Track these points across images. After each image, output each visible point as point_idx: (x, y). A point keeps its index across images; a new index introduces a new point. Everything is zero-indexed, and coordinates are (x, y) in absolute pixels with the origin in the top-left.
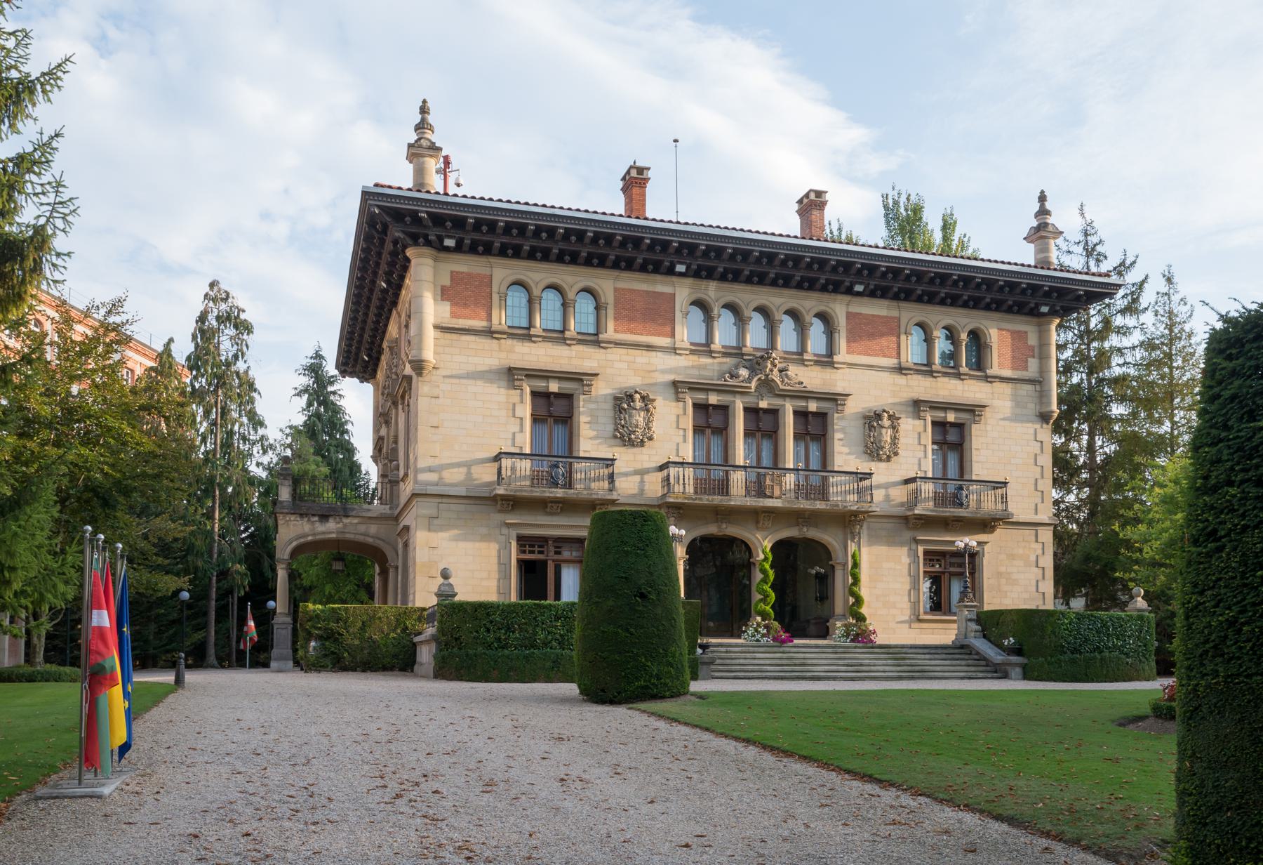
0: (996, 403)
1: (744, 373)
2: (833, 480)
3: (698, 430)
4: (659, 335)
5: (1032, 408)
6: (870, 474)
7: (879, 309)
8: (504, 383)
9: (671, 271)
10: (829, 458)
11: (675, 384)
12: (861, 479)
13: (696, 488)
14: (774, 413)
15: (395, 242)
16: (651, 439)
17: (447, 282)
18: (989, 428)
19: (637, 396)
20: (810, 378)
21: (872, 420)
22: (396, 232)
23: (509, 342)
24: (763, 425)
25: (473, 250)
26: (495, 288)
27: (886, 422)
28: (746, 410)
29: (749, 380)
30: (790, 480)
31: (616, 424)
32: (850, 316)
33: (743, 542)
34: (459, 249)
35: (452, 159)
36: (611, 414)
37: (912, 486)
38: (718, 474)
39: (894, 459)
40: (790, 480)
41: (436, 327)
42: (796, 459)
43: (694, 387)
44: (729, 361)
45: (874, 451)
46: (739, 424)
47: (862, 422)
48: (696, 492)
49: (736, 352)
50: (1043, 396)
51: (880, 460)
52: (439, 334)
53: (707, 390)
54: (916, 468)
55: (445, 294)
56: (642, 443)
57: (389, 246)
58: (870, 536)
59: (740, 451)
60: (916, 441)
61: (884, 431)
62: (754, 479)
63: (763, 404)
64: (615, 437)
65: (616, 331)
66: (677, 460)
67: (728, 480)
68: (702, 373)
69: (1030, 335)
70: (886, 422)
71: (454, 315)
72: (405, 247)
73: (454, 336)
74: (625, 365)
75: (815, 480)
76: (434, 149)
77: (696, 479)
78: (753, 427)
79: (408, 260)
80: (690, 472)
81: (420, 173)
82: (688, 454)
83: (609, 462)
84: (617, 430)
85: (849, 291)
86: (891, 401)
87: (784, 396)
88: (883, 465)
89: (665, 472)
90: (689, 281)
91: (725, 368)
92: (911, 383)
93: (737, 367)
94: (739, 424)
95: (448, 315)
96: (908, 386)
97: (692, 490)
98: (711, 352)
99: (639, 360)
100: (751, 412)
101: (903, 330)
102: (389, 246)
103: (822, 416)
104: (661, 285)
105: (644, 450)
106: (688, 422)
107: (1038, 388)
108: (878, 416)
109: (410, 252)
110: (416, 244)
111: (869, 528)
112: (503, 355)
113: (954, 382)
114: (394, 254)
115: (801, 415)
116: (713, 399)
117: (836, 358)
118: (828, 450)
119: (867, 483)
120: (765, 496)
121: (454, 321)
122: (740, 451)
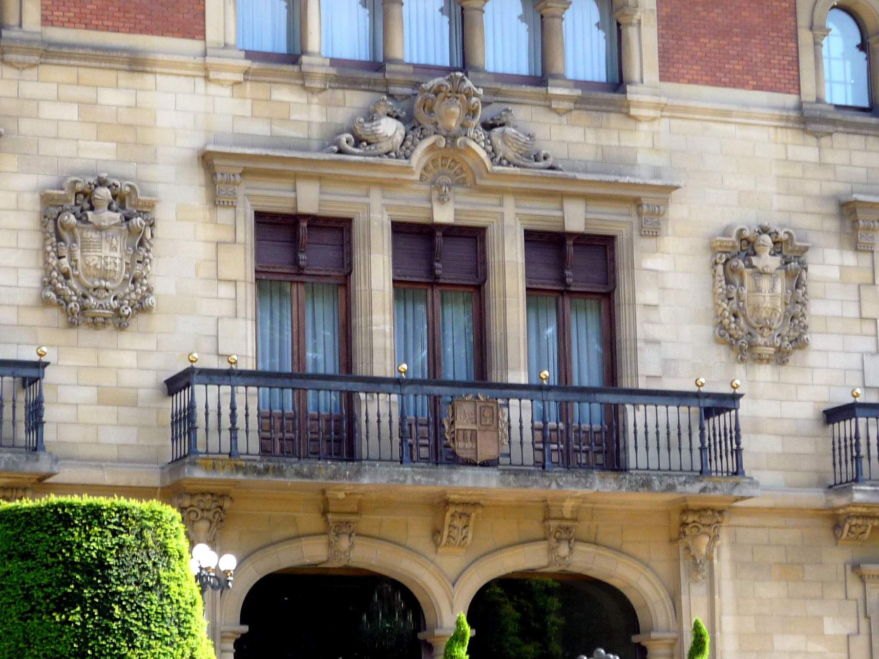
1: (389, 129)
2: (638, 417)
3: (267, 282)
4: (163, 32)
6: (735, 398)
10: (625, 356)
11: (207, 161)
12: (708, 413)
14: (473, 236)
16: (141, 308)
19: (104, 193)
20: (567, 137)
21: (735, 254)
24: (441, 260)
27: (768, 261)
28: (400, 229)
29: (405, 150)
30: (520, 413)
31: (47, 269)
33: (398, 586)
36: (31, 240)
37: (845, 428)
38: (324, 401)
39: (796, 357)
40: (520, 413)
42: (535, 363)
43: (255, 168)
44: (355, 100)
45: (739, 337)
46: (377, 269)
47: (705, 260)
48: (265, 451)
49: (372, 71)
51: (760, 359)
53: (296, 177)
54: (854, 380)
56: (119, 321)
58: (738, 565)
59: (384, 334)
60: (852, 311)
61: (765, 283)
62: (425, 415)
63: (444, 215)
64: (45, 303)
65: (46, 21)
66: (213, 363)
67: (351, 418)
70: (768, 261)
74: (71, 112)
75: (588, 415)
78: (418, 274)
80: (250, 399)
82: (242, 346)
83: (29, 374)
84: (48, 283)
86: (778, 202)
87: (501, 192)
88: (764, 373)
89: (183, 397)
92: (831, 157)
93: (370, 116)
94: (377, 269)
96: (822, 164)
97: (255, 447)
98: (303, 76)
100: (414, 236)
101: (803, 20)
103: (601, 247)
105: (126, 339)
106: (241, 263)
108: (747, 247)
111: (734, 544)
115: (544, 243)
116: (309, 199)
117: (634, 93)
118: (624, 332)
119: (723, 421)
120: (455, 461)
122: (384, 334)
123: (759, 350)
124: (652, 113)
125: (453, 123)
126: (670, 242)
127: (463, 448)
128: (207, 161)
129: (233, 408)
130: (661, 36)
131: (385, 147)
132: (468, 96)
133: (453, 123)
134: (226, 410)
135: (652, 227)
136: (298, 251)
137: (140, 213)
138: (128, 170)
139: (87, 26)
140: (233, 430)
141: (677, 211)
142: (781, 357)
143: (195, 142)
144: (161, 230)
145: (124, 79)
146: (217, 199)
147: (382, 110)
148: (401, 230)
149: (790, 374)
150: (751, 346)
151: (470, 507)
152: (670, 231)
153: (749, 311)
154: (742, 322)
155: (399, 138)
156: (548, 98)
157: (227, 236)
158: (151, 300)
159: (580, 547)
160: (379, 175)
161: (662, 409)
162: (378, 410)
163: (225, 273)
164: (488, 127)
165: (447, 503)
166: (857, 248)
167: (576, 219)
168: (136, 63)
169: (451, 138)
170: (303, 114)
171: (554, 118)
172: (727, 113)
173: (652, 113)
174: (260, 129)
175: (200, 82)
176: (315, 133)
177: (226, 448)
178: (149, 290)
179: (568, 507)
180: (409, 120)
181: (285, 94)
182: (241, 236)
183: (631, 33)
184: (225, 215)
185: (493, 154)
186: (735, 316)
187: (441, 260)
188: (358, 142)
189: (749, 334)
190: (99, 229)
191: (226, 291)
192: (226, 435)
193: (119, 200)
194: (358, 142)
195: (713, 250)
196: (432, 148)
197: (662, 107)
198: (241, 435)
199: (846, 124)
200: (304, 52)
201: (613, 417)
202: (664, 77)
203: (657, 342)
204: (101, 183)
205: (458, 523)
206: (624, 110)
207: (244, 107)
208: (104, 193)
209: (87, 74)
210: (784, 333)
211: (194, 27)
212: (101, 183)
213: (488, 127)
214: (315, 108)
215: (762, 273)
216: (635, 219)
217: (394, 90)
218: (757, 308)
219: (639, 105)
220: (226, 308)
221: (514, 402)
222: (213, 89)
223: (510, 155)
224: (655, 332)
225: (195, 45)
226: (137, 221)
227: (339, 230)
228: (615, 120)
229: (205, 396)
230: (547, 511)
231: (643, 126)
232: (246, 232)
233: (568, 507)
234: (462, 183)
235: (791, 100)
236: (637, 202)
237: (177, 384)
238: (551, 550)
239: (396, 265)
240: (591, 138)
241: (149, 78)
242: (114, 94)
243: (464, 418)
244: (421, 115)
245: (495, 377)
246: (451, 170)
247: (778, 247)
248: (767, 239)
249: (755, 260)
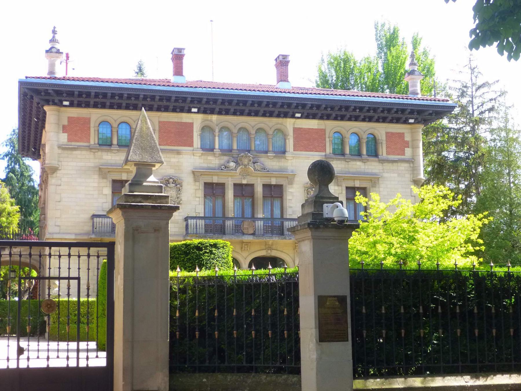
0: (386, 175)
1: (232, 164)
4: (185, 146)
5: (408, 177)
7: (313, 124)
8: (96, 176)
9: (189, 111)
10: (284, 210)
13: (205, 230)
15: (38, 104)
17: (66, 123)
18: (381, 189)
19: (171, 180)
22: (36, 100)
23: (100, 153)
25: (79, 105)
26: (92, 125)
30: (260, 224)
32: (296, 130)
34: (72, 105)
35: (70, 56)
41: (60, 147)
44: (226, 158)
46: (230, 194)
47: (304, 189)
50: (414, 170)
52: (60, 151)
53: (212, 175)
55: (65, 129)
57: (35, 105)
63: (244, 182)
67: (224, 226)
68: (209, 165)
69: (406, 135)
71: (69, 140)
72: (43, 106)
73: (69, 152)
76: (58, 52)
77: (205, 225)
79: (45, 113)
80: (201, 223)
81: (52, 66)
82: (200, 211)
85: (293, 116)
90: (200, 116)
91: (222, 162)
93: (228, 162)
94: (230, 194)
95: (66, 140)
98: (214, 154)
99: (173, 160)
102: (35, 105)
104: (185, 118)
106: (201, 193)
107: (412, 165)
109: (46, 108)
110: (48, 104)
112: (97, 160)
113: (359, 163)
114: (38, 108)
116: (215, 180)
121: (70, 143)
124: (291, 158)
125: (246, 163)
126: (295, 186)
127: (245, 231)
128: (193, 172)
130: (294, 141)
131: (231, 168)
132: (249, 157)
133: (246, 163)
135: (291, 183)
136: (213, 190)
137: (179, 184)
138: (177, 175)
139: (169, 145)
140: (196, 229)
141: (297, 179)
143: (191, 168)
144: (183, 187)
145: (176, 156)
146: (195, 181)
147: (231, 160)
148: (235, 185)
151: (248, 243)
155: (234, 166)
156: (268, 156)
157: (198, 188)
158: (181, 202)
159: (273, 251)
160: (230, 174)
161: (289, 222)
162: (229, 223)
163: (198, 196)
164: (254, 163)
165: (243, 242)
166: (338, 186)
167: (274, 182)
168: (178, 153)
169: (245, 166)
170: (214, 161)
171: (270, 160)
172: (309, 157)
173: (291, 158)
174: (205, 165)
175: (192, 156)
176: (217, 166)
177: (195, 232)
178: (181, 200)
179: (270, 243)
180: (236, 162)
181: (210, 158)
182: (201, 188)
183: (287, 141)
184: (197, 183)
185: (255, 169)
187: (244, 191)
188: (226, 167)
190: (170, 188)
191: (197, 199)
192: (195, 230)
193: (174, 182)
194: (226, 167)
196: (241, 168)
197: (294, 157)
198: (198, 229)
199: (336, 159)
200: (214, 149)
201: (282, 223)
202: (294, 150)
204: (171, 178)
205: (246, 246)
206: (285, 158)
207: (202, 161)
208: (171, 180)
209: (168, 155)
211: (191, 145)
212: (171, 178)
213: (254, 163)
214: (217, 160)
216: (287, 181)
217: (234, 156)
219: (288, 157)
220: (197, 203)
221: (257, 222)
222: (195, 157)
223: (259, 169)
224: (291, 205)
225: (191, 148)
226: (178, 186)
227: (222, 186)
228: (283, 160)
229: (191, 222)
230: (266, 244)
231: (289, 161)
232: (202, 187)
233: (270, 243)
234: (249, 175)
235: (324, 154)
236: (287, 177)
237: (186, 219)
238: (267, 251)
239: (234, 193)
240: (278, 164)
241: (181, 156)
242: (174, 159)
243: (246, 225)
244: (239, 161)
245: (256, 216)
246: (245, 173)
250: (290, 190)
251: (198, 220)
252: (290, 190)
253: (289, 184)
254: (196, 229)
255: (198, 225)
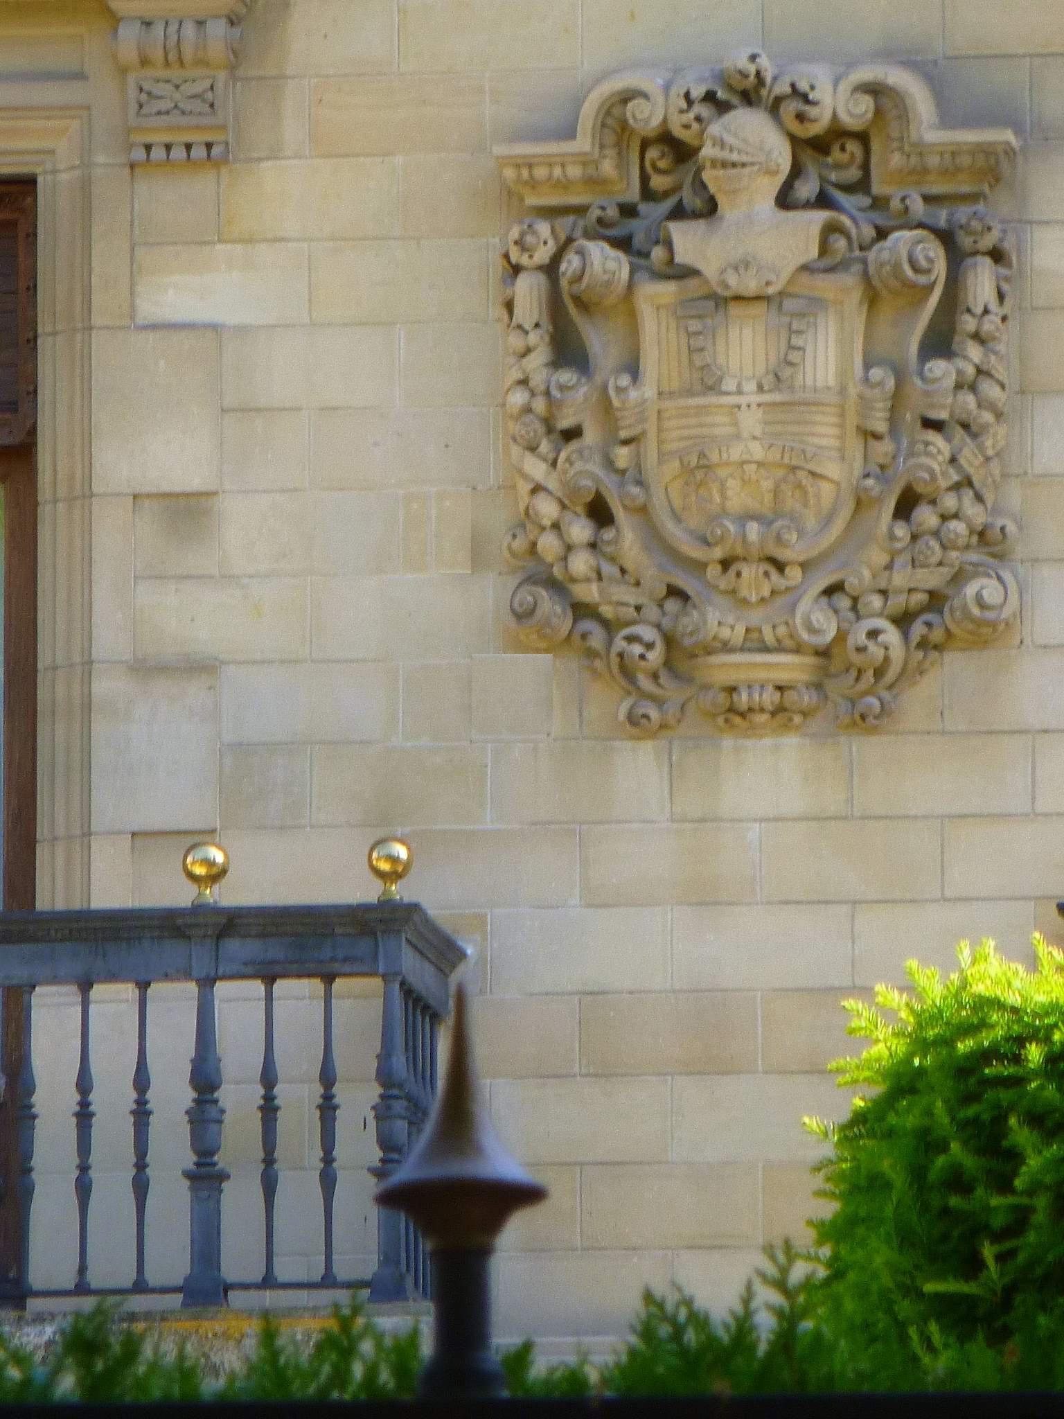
45: (624, 614)
51: (734, 713)
61: (744, 347)
123: (723, 669)
126: (288, 188)
129: (205, 1080)
134: (173, 1094)
142: (848, 695)
149: (912, 774)
150: (679, 654)
152: (292, 131)
153: (665, 478)
154: (627, 538)
186: (599, 513)
189: (674, 592)
195: (513, 196)
203: (200, 667)
210: (860, 577)
215: (724, 302)
218: (699, 469)
224: (191, 616)
247: (832, 163)
248: (756, 139)
249: (688, 241)
250: (175, 295)
251: (238, 1000)
252: (175, 295)
253: (144, 160)
254: (206, 1177)
255: (238, 1098)
